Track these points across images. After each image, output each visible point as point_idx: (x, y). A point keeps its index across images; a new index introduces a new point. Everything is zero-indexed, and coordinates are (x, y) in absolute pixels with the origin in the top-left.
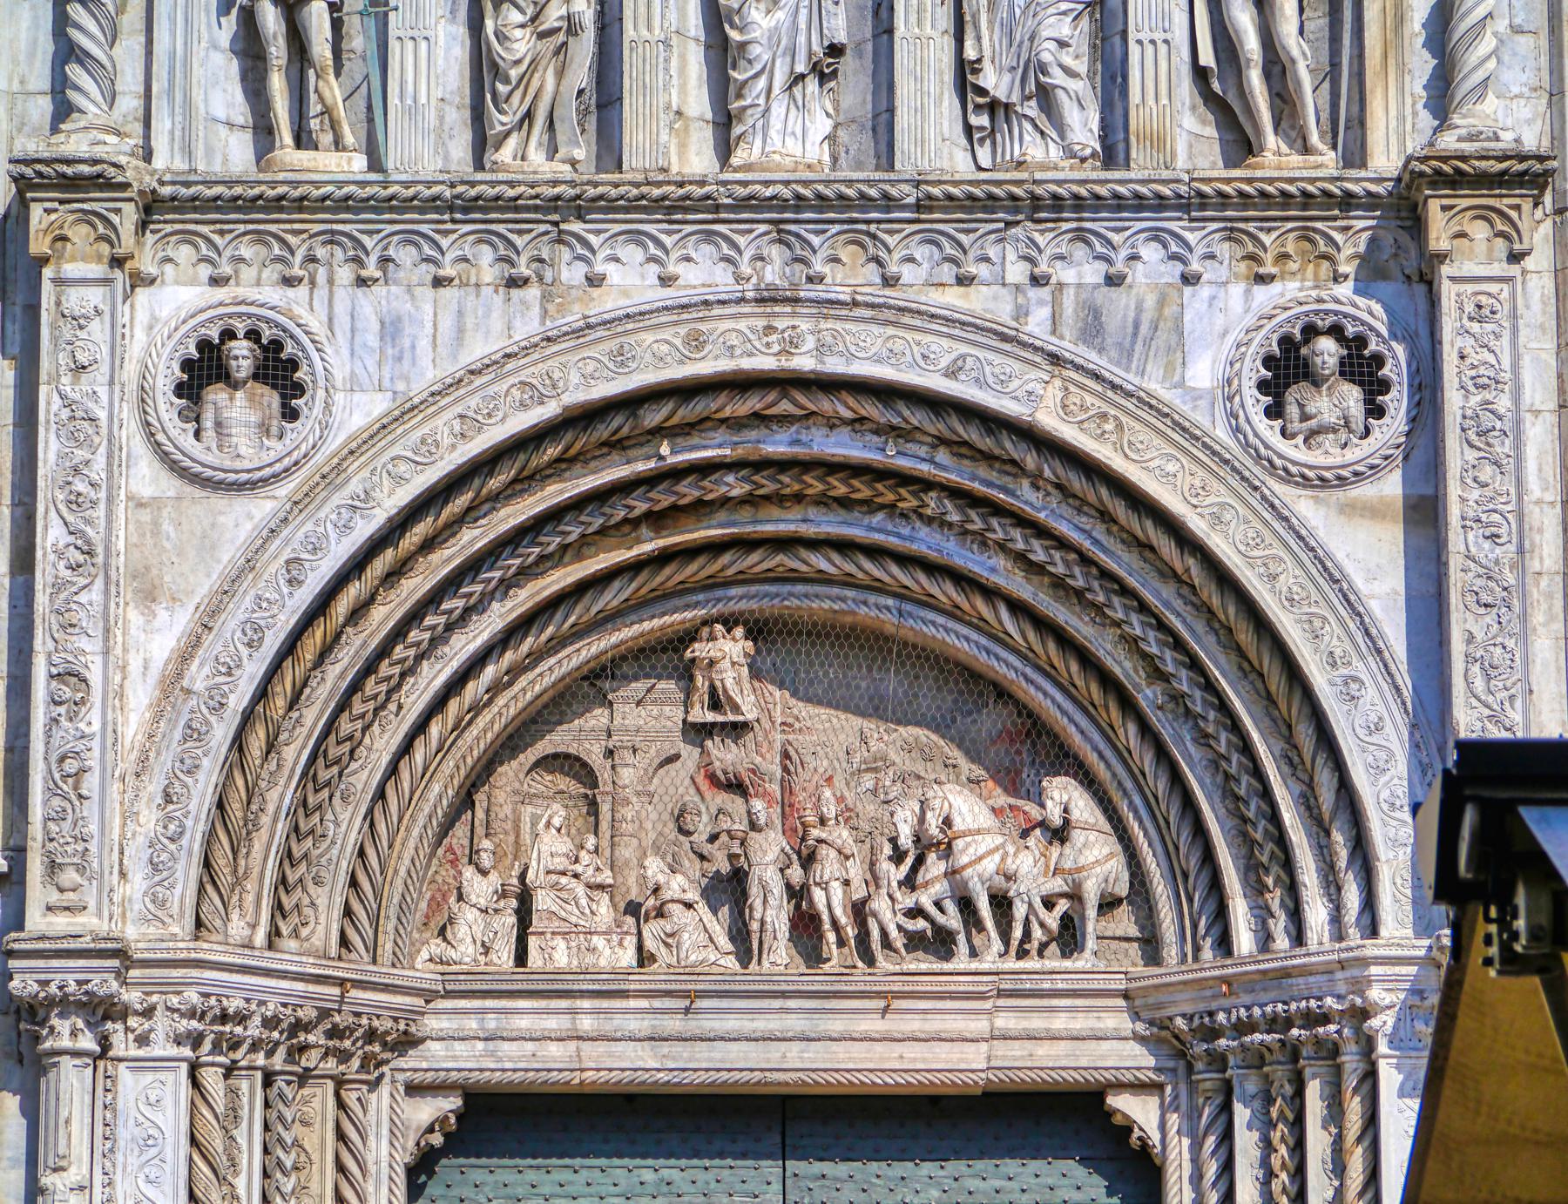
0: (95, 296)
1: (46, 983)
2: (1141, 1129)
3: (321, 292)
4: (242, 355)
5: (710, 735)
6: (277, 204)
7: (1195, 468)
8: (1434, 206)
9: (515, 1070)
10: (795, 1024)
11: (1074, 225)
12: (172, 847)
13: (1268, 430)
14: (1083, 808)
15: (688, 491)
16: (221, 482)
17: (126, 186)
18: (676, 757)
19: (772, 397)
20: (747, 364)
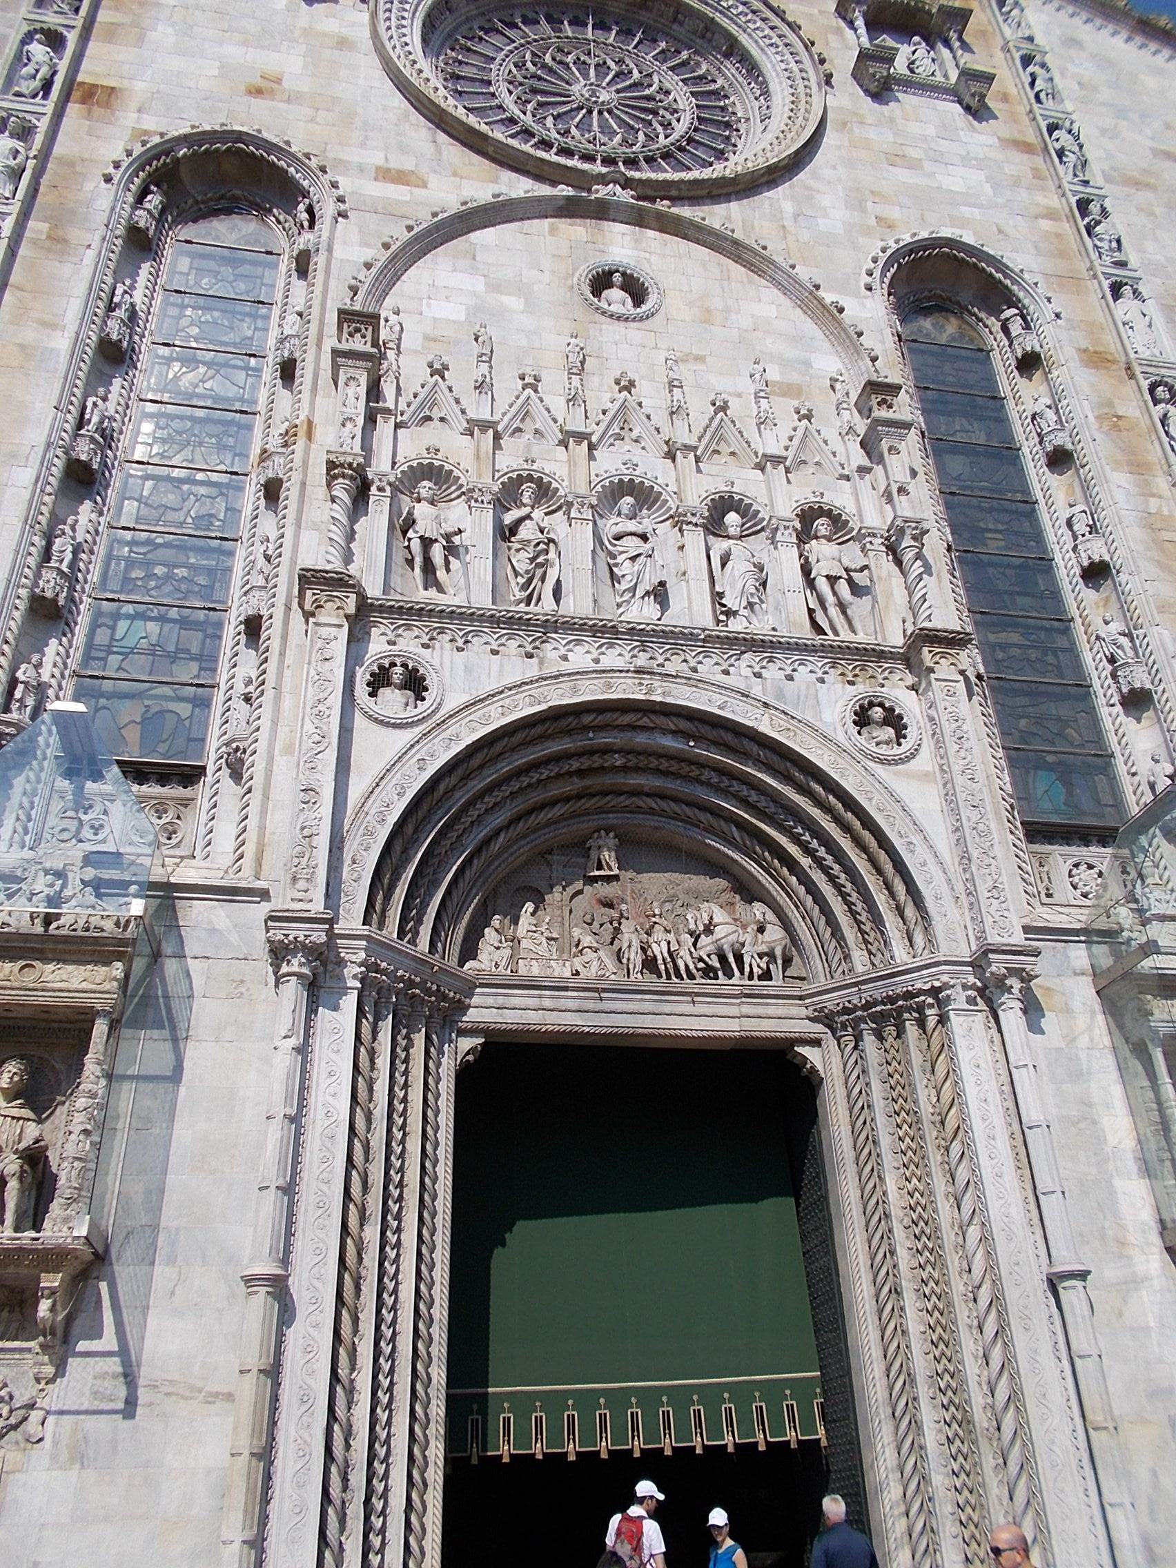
0: (334, 631)
1: (287, 936)
3: (437, 652)
4: (397, 673)
8: (925, 650)
12: (355, 884)
13: (861, 739)
14: (771, 916)
15: (597, 761)
19: (639, 715)
20: (632, 696)
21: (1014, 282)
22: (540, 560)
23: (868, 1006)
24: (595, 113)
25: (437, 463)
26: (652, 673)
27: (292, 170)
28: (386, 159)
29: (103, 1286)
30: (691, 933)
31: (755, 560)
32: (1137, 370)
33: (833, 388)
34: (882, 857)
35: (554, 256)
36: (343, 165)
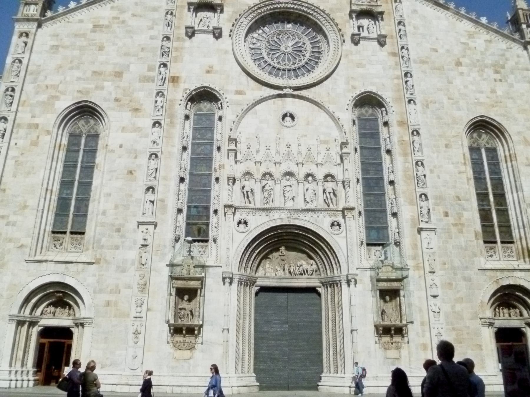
4: (243, 221)
6: (246, 209)
10: (289, 281)
14: (314, 262)
21: (384, 102)
22: (269, 194)
23: (329, 282)
29: (202, 328)
30: (298, 266)
31: (314, 189)
32: (410, 127)
33: (335, 141)
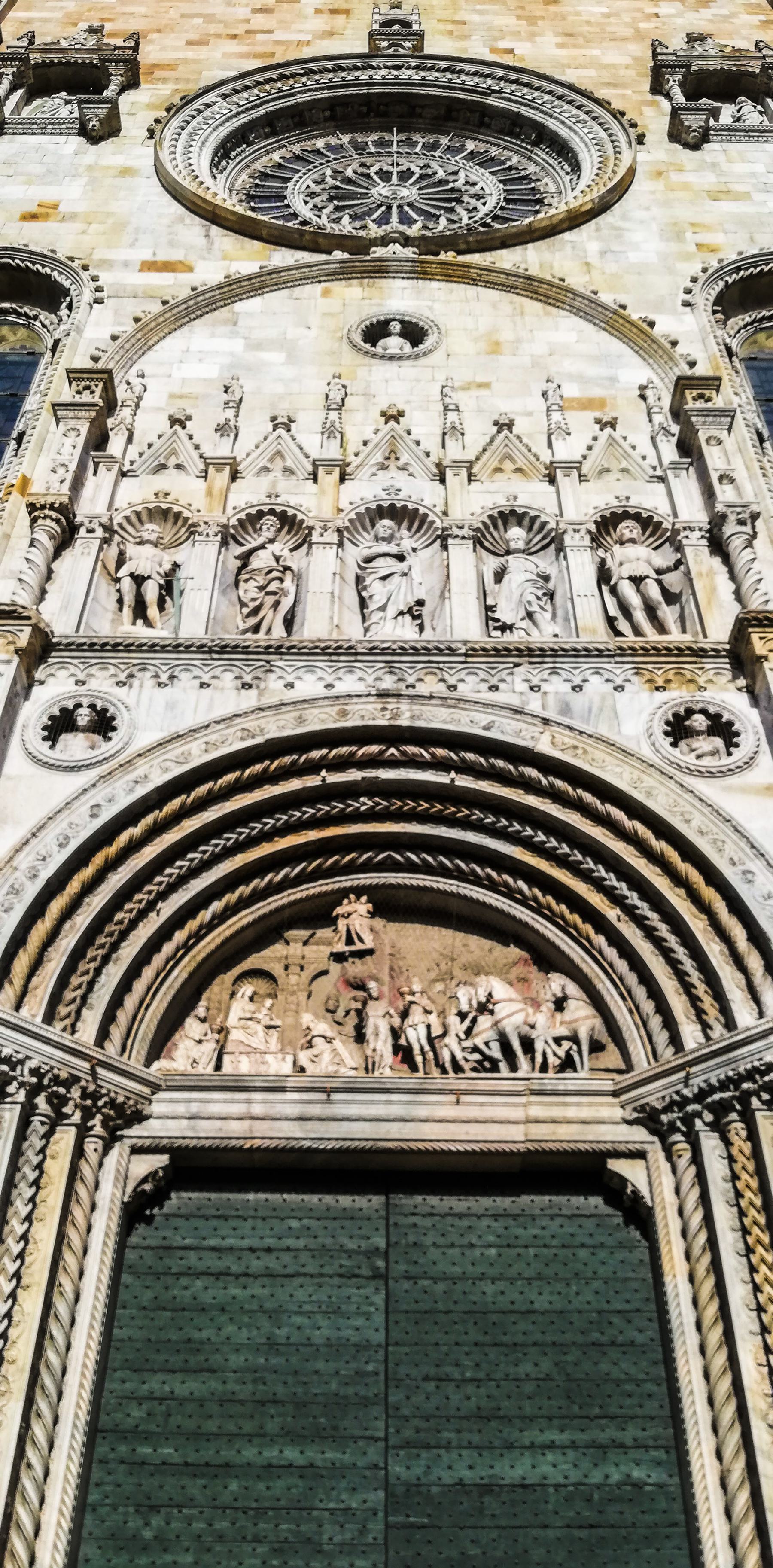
2: (633, 1185)
5: (346, 960)
6: (115, 647)
7: (633, 770)
8: (755, 638)
9: (207, 1138)
10: (396, 1111)
11: (551, 665)
14: (573, 989)
16: (60, 766)
17: (28, 618)
18: (325, 973)
20: (371, 723)
22: (273, 587)
23: (701, 1096)
24: (395, 210)
25: (164, 506)
26: (399, 696)
27: (55, 274)
28: (154, 254)
30: (462, 1016)
34: (709, 894)
35: (324, 314)
36: (106, 264)
